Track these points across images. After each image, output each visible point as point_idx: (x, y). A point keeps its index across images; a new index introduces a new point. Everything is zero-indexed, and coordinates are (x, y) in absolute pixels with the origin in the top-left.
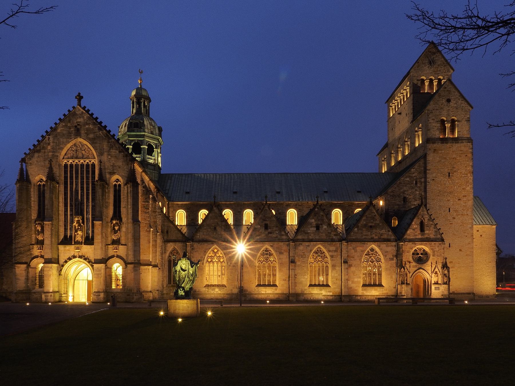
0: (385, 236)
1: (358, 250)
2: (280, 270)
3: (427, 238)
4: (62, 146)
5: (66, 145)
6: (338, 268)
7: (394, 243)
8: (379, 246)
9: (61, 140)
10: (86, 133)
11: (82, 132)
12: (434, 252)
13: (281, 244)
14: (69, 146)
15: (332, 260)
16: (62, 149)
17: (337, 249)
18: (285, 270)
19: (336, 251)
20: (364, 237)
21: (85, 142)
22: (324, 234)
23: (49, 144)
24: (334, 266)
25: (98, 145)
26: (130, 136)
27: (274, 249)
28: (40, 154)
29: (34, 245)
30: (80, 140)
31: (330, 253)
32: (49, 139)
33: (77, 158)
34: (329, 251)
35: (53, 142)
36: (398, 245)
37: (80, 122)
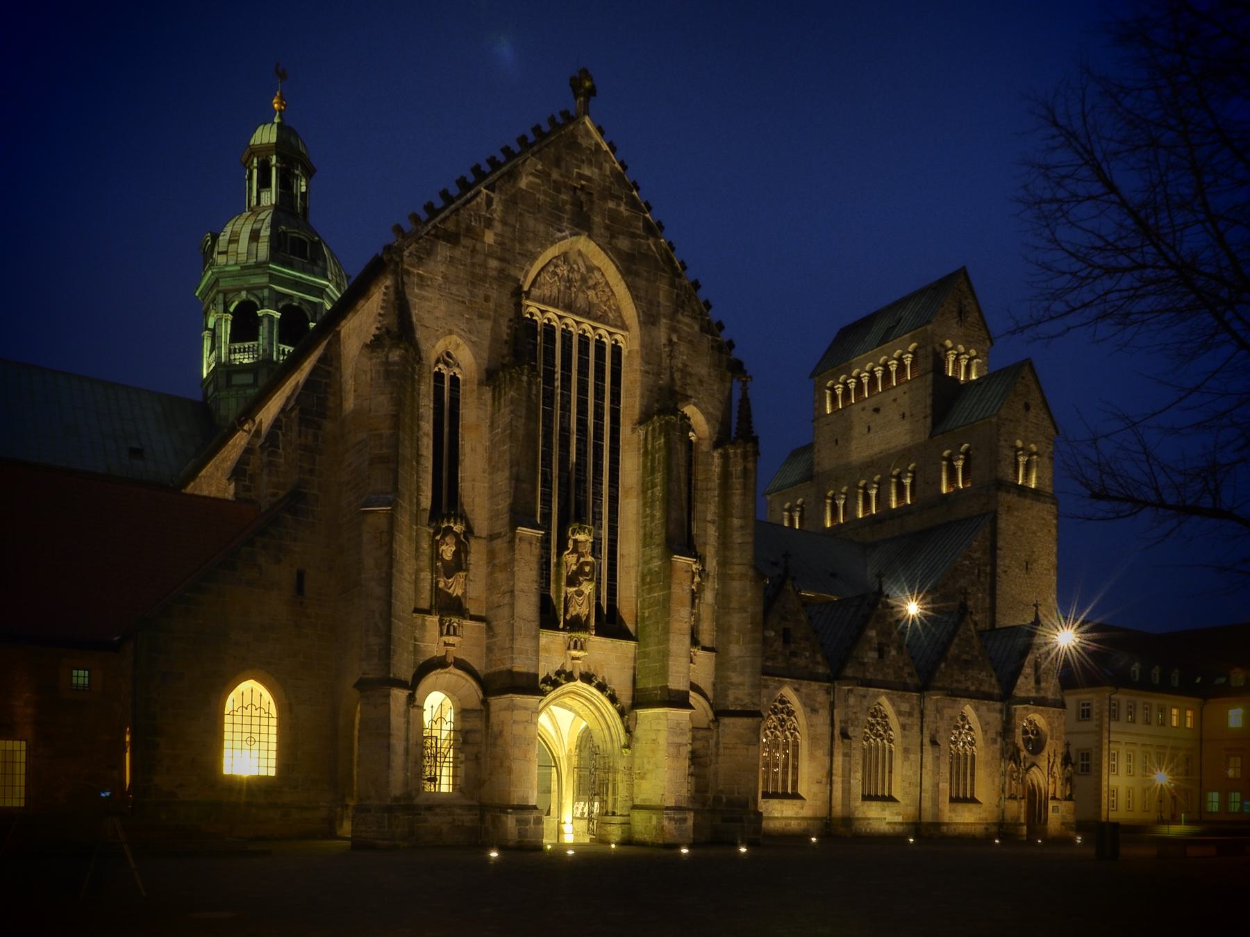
0: (985, 688)
1: (946, 716)
2: (812, 756)
3: (1043, 698)
4: (530, 247)
5: (544, 247)
6: (915, 757)
7: (998, 705)
8: (976, 709)
9: (531, 223)
10: (607, 228)
11: (597, 219)
12: (1052, 731)
13: (815, 685)
14: (552, 252)
15: (904, 736)
16: (533, 257)
17: (912, 708)
18: (821, 754)
19: (910, 714)
20: (955, 685)
21: (600, 259)
22: (891, 671)
23: (489, 223)
24: (906, 751)
25: (641, 283)
26: (274, 279)
27: (800, 697)
28: (458, 253)
29: (428, 612)
30: (585, 245)
31: (901, 719)
32: (489, 202)
33: (569, 307)
34: (899, 713)
35: (504, 223)
36: (1008, 709)
37: (589, 179)
